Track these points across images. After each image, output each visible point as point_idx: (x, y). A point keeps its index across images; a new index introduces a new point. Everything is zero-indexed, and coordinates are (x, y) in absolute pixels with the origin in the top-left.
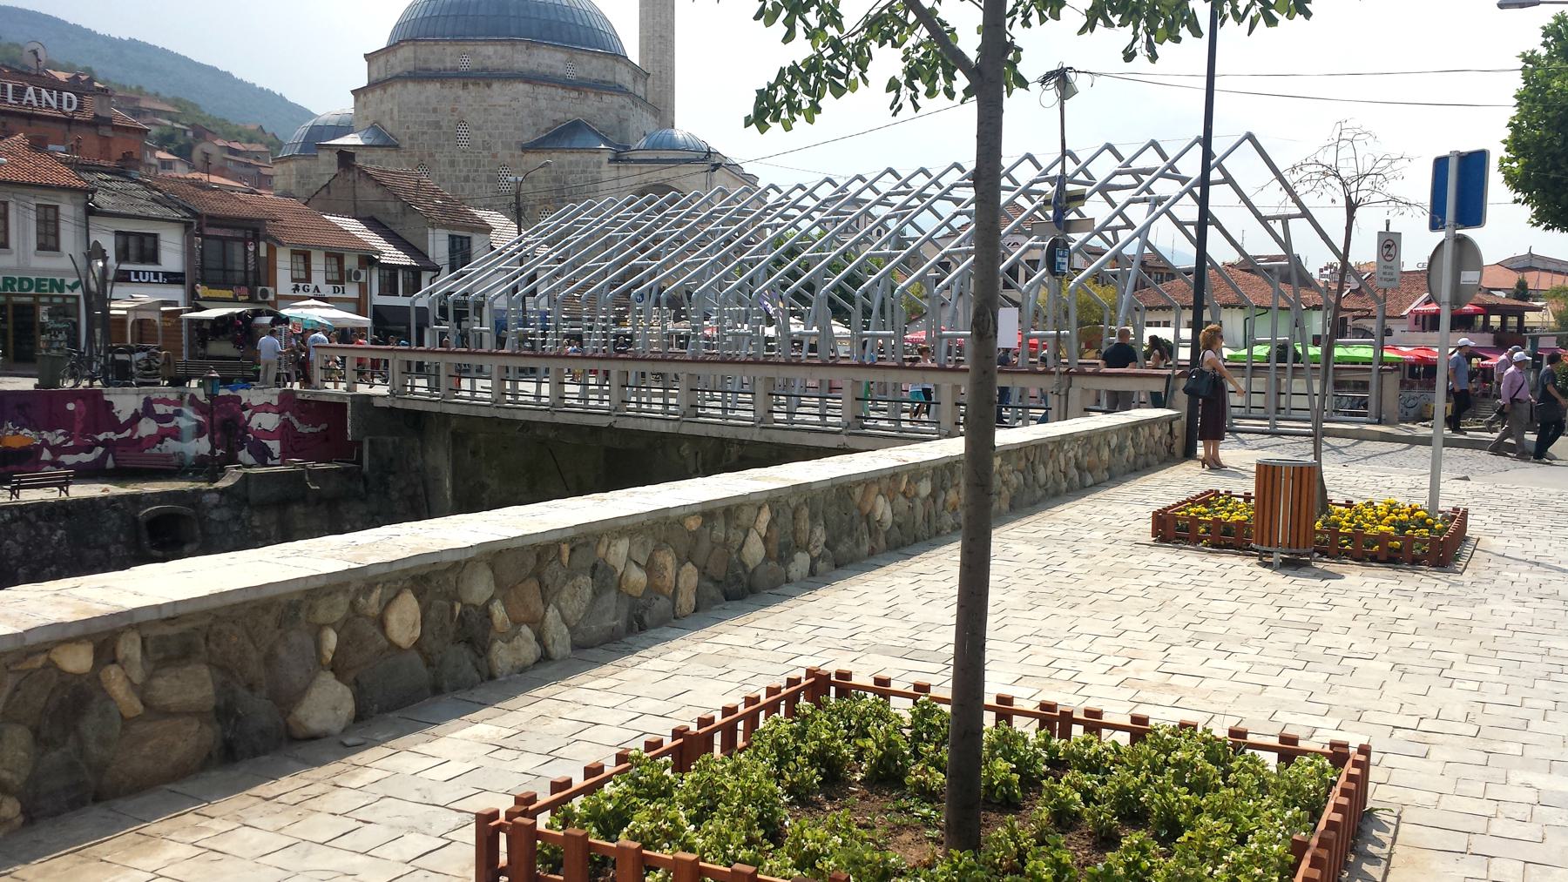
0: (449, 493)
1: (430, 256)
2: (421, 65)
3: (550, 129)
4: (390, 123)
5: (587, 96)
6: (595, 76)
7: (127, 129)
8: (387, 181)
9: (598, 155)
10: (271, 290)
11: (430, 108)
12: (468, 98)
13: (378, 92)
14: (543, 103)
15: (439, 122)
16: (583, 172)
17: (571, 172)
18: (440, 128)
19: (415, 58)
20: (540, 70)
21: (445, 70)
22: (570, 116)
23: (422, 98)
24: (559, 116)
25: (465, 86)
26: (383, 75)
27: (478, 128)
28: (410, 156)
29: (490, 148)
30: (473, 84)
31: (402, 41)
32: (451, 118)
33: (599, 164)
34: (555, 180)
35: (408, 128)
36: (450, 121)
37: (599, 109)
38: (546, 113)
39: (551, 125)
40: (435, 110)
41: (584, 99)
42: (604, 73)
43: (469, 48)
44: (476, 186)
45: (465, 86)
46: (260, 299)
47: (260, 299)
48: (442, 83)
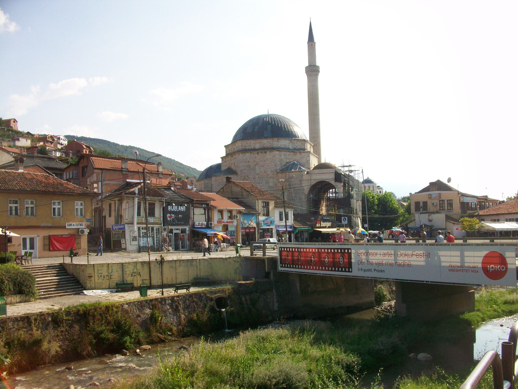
0: (298, 289)
1: (257, 209)
2: (244, 148)
4: (234, 167)
6: (298, 147)
7: (166, 174)
8: (242, 185)
10: (212, 223)
11: (247, 161)
12: (259, 157)
13: (230, 157)
14: (283, 157)
15: (250, 165)
16: (297, 178)
18: (250, 167)
19: (242, 146)
20: (282, 146)
21: (251, 148)
22: (291, 160)
23: (245, 158)
24: (288, 161)
25: (258, 153)
26: (231, 152)
27: (263, 166)
28: (241, 177)
29: (266, 173)
30: (261, 152)
31: (238, 141)
32: (254, 164)
33: (302, 175)
35: (240, 168)
36: (253, 165)
37: (301, 158)
40: (248, 162)
41: (295, 155)
45: (258, 153)
46: (210, 226)
47: (210, 226)
48: (251, 153)
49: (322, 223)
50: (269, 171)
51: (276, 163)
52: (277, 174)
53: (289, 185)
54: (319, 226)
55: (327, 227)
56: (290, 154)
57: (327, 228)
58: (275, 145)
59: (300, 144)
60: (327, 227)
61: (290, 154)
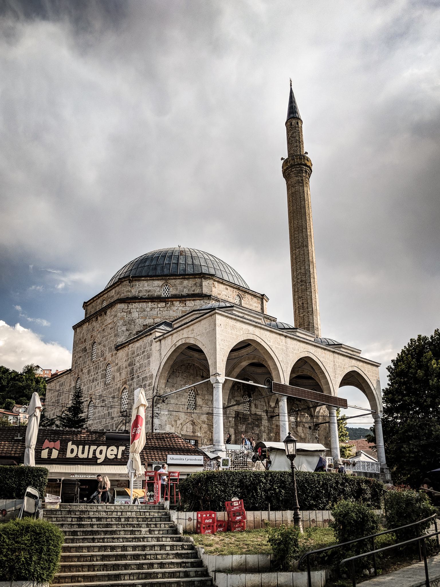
3: (140, 331)
5: (173, 305)
6: (185, 292)
9: (151, 336)
15: (86, 347)
16: (144, 352)
17: (138, 355)
18: (86, 351)
20: (141, 295)
22: (158, 320)
27: (100, 344)
28: (75, 374)
30: (101, 315)
34: (129, 365)
38: (137, 321)
39: (142, 328)
41: (170, 307)
42: (193, 289)
43: (105, 296)
44: (97, 383)
45: (97, 318)
49: (70, 446)
50: (108, 350)
51: (117, 331)
52: (116, 354)
53: (132, 372)
54: (55, 454)
55: (99, 461)
56: (154, 306)
57: (101, 464)
58: (125, 294)
59: (190, 285)
60: (99, 461)
61: (155, 306)
